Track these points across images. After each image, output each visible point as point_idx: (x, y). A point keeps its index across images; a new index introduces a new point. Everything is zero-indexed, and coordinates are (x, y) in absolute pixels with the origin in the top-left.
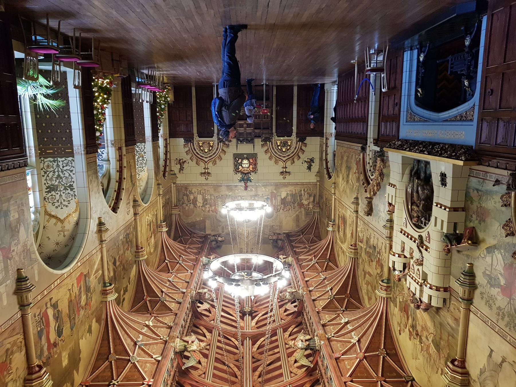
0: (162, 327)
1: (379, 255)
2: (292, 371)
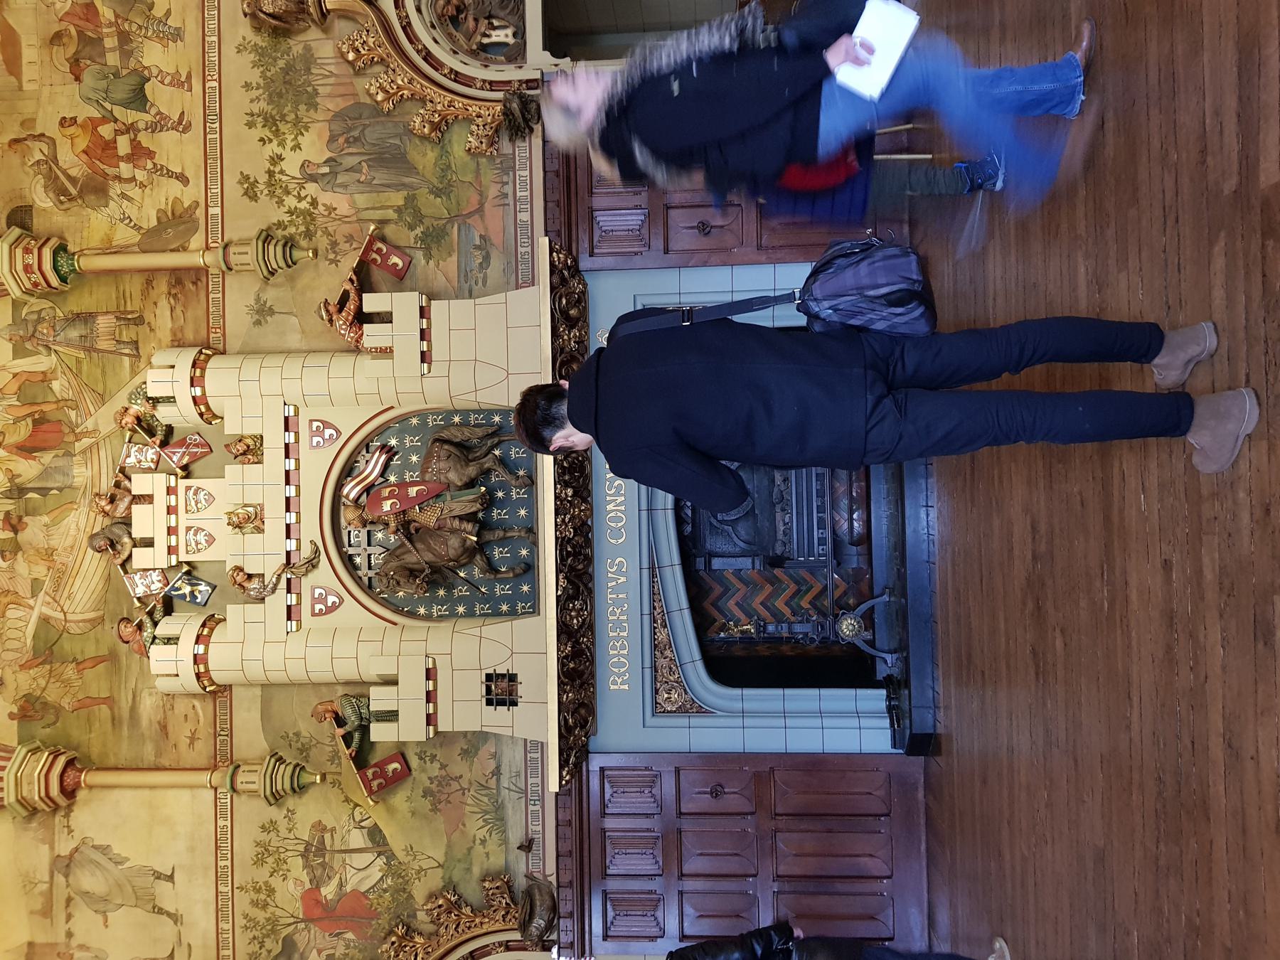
1: (123, 146)
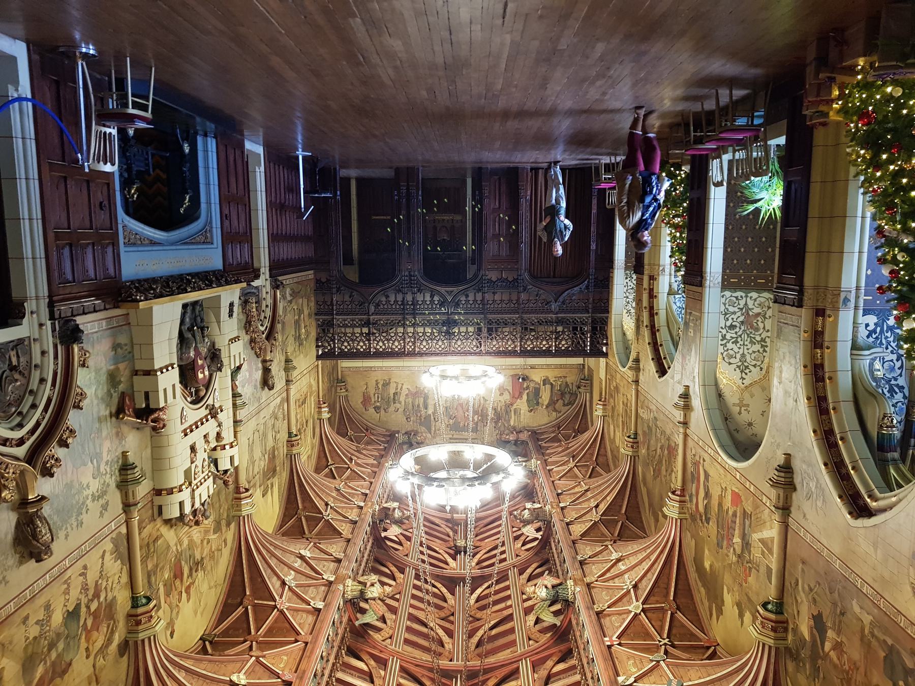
0: (326, 560)
2: (532, 637)
